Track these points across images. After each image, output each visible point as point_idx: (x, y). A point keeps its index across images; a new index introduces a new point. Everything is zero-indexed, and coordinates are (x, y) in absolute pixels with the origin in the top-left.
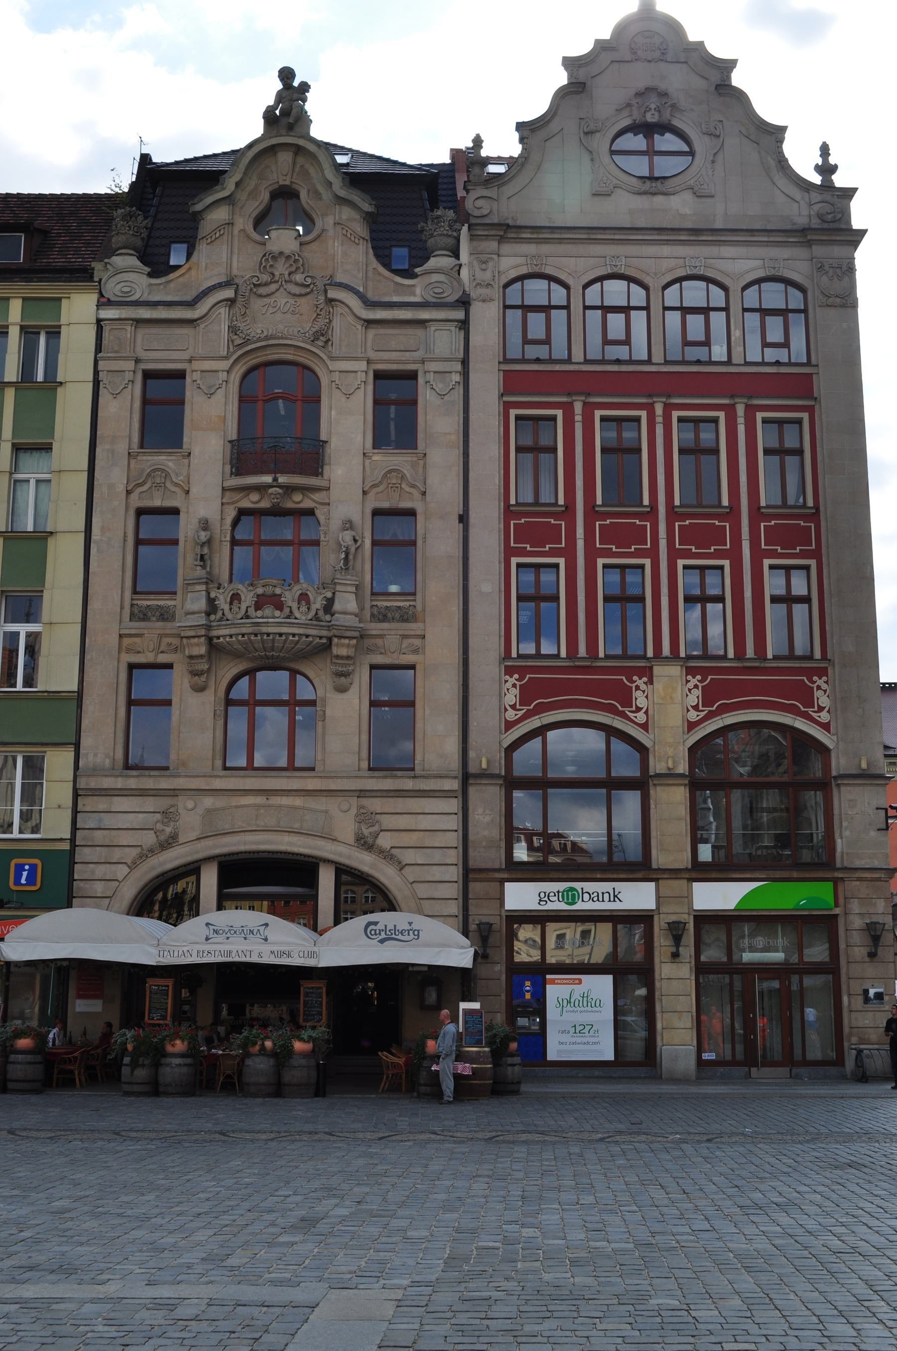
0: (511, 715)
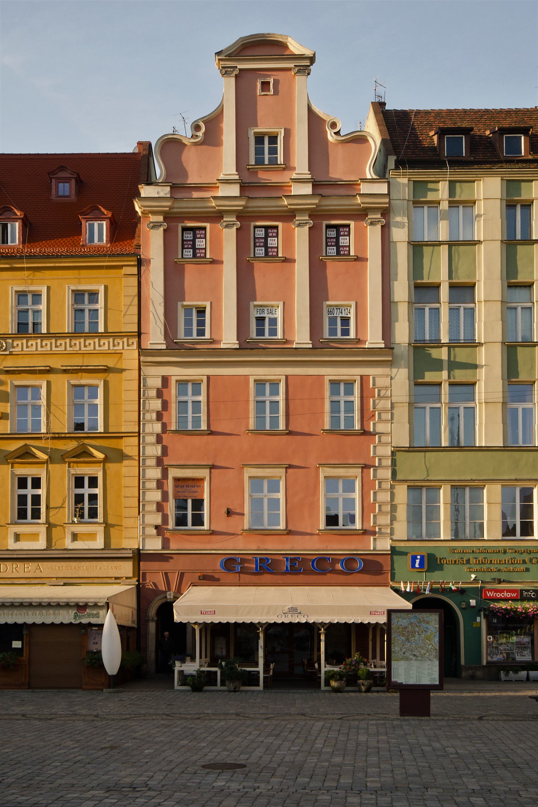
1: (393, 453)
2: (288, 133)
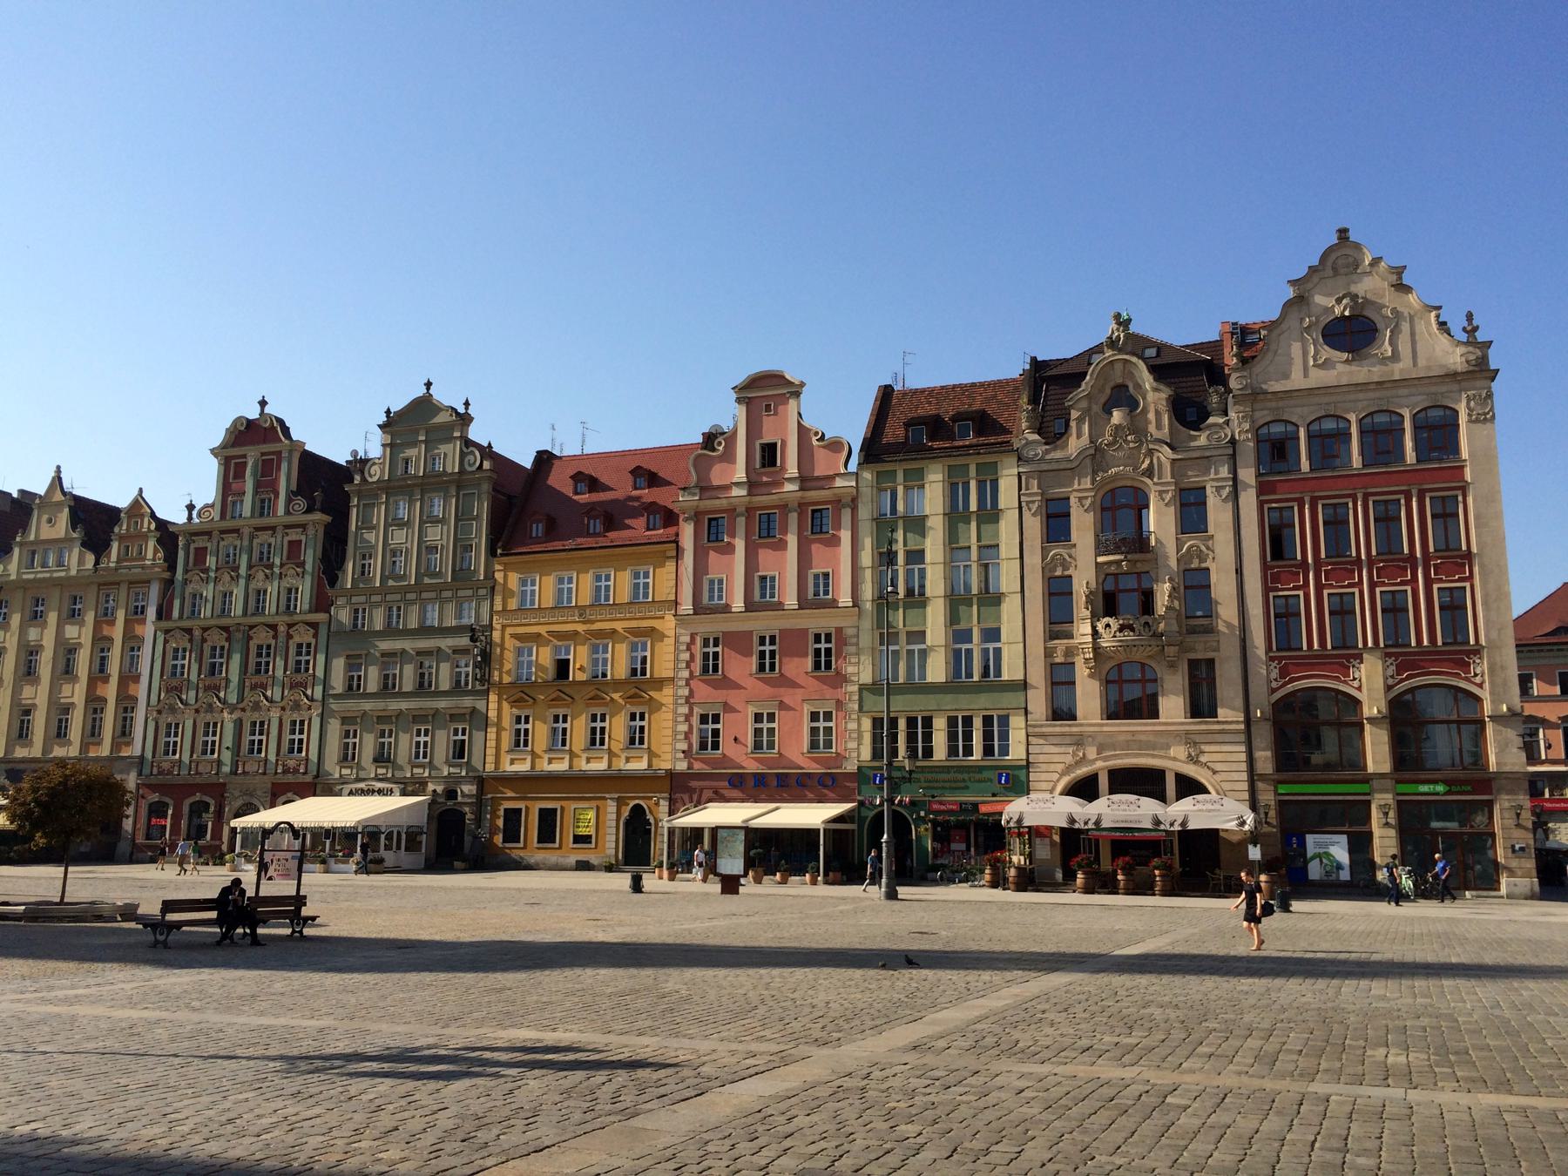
0: (1274, 685)
1: (860, 690)
2: (784, 443)
